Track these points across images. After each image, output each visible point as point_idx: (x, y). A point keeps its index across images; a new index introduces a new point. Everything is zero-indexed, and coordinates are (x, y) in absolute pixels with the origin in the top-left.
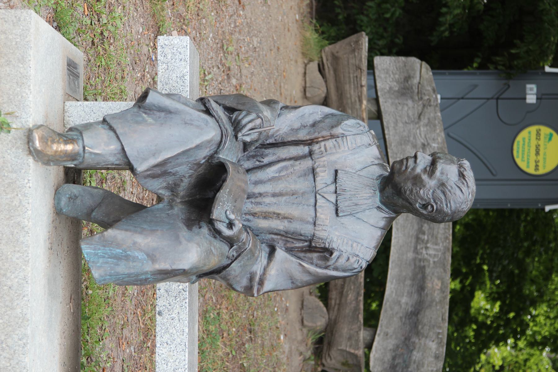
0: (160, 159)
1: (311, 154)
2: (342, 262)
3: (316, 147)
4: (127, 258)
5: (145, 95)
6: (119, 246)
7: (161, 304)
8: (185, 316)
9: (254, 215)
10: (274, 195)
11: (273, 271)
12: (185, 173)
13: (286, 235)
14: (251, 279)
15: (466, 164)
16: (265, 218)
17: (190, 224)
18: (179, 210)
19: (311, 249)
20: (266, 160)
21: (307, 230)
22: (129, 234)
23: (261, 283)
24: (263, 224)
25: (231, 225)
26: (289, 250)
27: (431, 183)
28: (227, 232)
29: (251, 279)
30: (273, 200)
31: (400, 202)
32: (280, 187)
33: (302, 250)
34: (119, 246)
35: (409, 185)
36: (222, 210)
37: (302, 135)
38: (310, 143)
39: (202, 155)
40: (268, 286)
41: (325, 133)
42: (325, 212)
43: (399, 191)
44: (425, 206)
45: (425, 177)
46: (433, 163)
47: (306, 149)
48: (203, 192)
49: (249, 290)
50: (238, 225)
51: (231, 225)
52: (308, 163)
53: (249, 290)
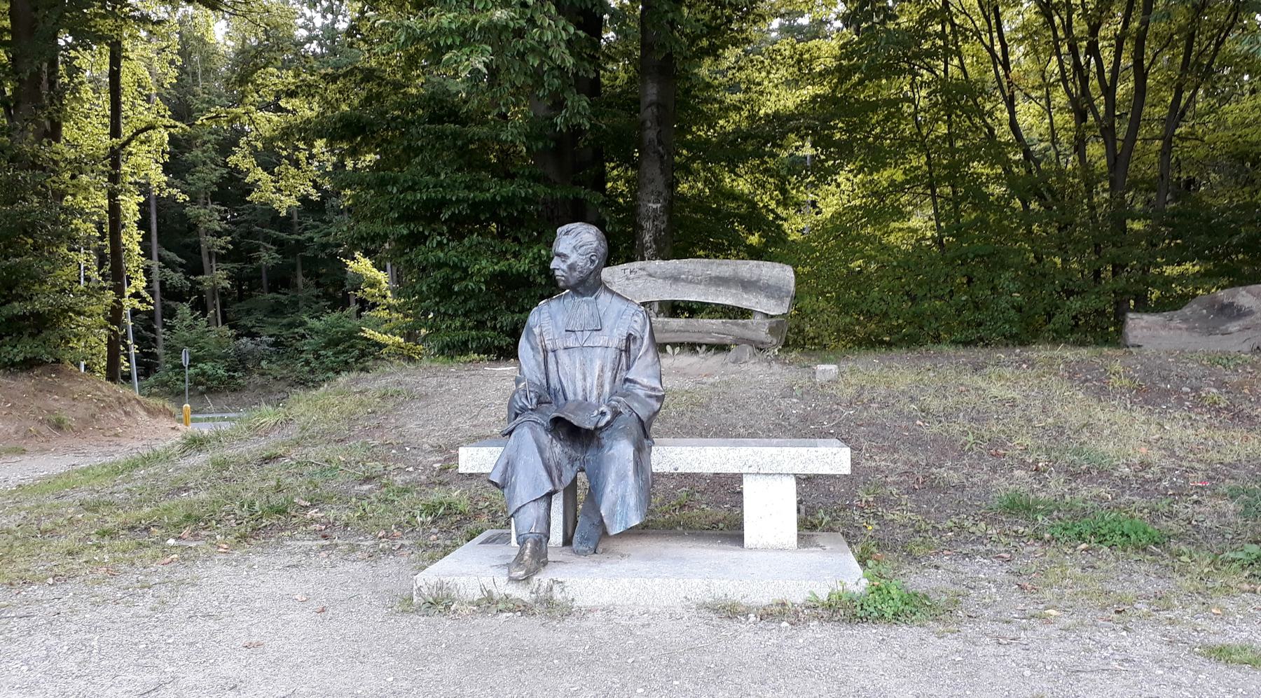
0: (544, 474)
1: (554, 351)
2: (637, 327)
3: (549, 347)
4: (623, 497)
5: (496, 485)
6: (615, 504)
7: (668, 469)
8: (678, 449)
9: (599, 395)
10: (585, 379)
11: (645, 381)
12: (557, 450)
13: (616, 370)
14: (650, 396)
15: (559, 230)
16: (602, 386)
17: (600, 447)
18: (589, 456)
19: (627, 350)
20: (558, 387)
21: (611, 354)
22: (604, 498)
23: (654, 389)
24: (607, 388)
25: (603, 414)
26: (628, 368)
27: (573, 258)
28: (608, 417)
29: (650, 396)
30: (589, 380)
31: (591, 280)
32: (579, 376)
33: (628, 358)
34: (615, 504)
35: (576, 274)
36: (585, 421)
37: (541, 359)
38: (545, 351)
39: (546, 439)
40: (656, 384)
41: (538, 340)
42: (599, 340)
43: (582, 282)
44: (592, 262)
45: (569, 262)
46: (559, 255)
47: (550, 354)
48: (576, 435)
49: (660, 399)
50: (604, 408)
51: (603, 414)
52: (561, 353)
53: (660, 399)
